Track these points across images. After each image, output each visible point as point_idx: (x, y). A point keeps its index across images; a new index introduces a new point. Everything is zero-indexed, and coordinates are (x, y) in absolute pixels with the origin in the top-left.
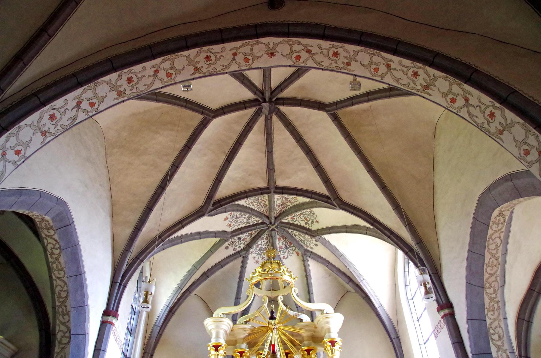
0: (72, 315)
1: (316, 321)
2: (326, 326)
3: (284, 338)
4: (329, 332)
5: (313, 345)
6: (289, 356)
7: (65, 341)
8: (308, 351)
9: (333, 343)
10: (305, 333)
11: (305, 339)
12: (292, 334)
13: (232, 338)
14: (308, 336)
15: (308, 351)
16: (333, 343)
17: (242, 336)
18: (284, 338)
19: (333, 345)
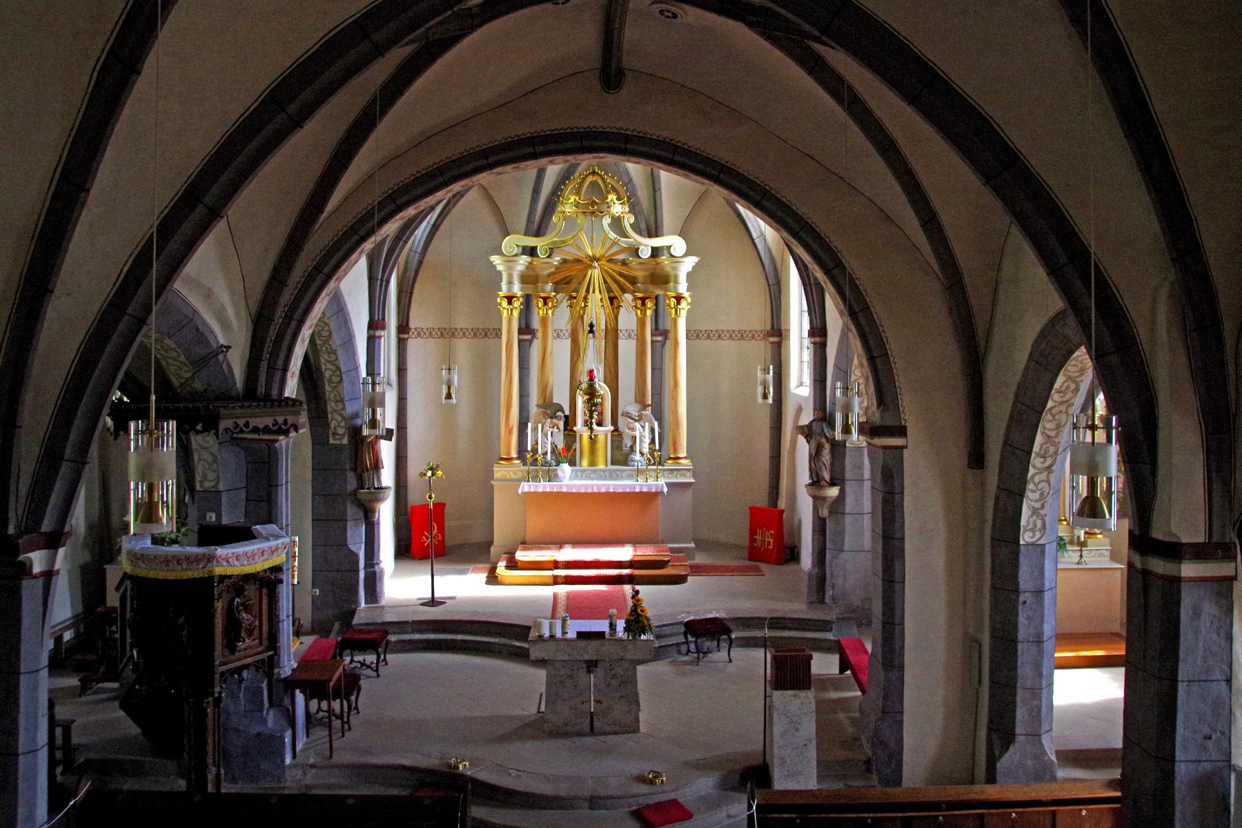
0: (339, 353)
1: (659, 260)
2: (672, 273)
3: (609, 280)
4: (676, 282)
5: (651, 288)
6: (615, 301)
7: (335, 379)
8: (643, 300)
9: (679, 299)
10: (639, 274)
11: (640, 280)
12: (621, 274)
13: (531, 273)
14: (645, 276)
15: (643, 300)
16: (679, 299)
17: (546, 273)
18: (609, 280)
19: (679, 303)
